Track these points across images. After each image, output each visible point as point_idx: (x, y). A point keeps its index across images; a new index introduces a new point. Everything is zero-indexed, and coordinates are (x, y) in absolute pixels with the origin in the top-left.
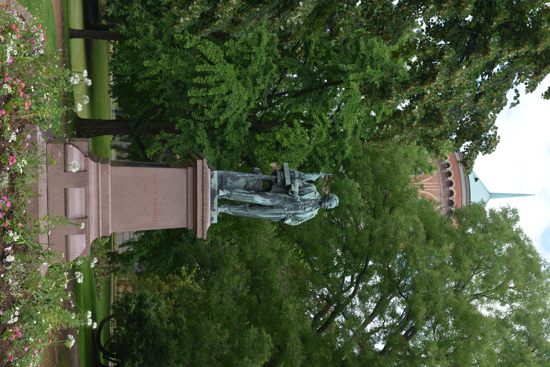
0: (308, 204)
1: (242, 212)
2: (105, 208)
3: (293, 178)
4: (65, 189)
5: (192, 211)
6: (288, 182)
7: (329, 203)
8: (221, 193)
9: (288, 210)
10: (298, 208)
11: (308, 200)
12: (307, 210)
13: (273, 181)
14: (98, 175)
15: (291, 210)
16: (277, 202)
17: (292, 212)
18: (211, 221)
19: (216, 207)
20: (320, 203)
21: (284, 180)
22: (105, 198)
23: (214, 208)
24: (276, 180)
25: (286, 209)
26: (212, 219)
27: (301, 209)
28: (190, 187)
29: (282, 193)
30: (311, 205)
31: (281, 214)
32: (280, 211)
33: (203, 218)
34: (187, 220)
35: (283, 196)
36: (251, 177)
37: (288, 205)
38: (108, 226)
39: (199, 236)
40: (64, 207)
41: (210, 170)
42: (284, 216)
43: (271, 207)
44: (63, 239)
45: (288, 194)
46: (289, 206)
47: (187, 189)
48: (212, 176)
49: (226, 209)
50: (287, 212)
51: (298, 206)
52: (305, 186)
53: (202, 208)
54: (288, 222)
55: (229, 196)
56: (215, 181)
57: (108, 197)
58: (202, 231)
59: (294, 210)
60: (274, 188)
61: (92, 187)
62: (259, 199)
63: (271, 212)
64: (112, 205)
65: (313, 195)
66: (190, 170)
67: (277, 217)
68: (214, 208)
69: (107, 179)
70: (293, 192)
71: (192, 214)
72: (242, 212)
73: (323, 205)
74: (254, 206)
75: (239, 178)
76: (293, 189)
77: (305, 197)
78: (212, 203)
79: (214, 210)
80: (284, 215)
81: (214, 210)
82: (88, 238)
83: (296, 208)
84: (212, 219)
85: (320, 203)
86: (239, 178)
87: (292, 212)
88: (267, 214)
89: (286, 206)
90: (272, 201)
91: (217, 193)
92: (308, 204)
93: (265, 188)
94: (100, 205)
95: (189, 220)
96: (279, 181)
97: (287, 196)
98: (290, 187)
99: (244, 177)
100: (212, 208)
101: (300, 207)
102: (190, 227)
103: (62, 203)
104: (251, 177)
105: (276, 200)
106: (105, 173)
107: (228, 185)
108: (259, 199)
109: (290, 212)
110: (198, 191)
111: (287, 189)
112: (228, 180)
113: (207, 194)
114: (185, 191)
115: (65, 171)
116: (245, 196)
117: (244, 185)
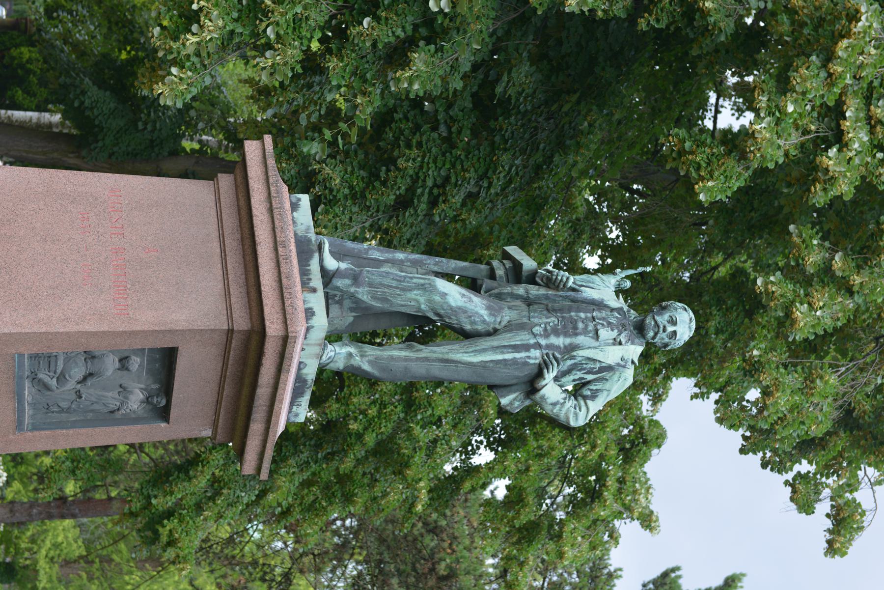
0: (604, 319)
1: (403, 353)
5: (242, 280)
7: (666, 316)
9: (546, 335)
10: (575, 328)
15: (556, 332)
17: (560, 341)
18: (308, 319)
23: (312, 284)
25: (537, 330)
27: (585, 332)
28: (230, 221)
30: (613, 321)
31: (527, 348)
33: (280, 281)
37: (541, 321)
41: (285, 188)
46: (545, 320)
47: (223, 251)
48: (295, 206)
50: (543, 342)
51: (574, 323)
53: (272, 256)
58: (280, 316)
59: (566, 335)
63: (495, 343)
66: (225, 181)
67: (514, 361)
68: (312, 284)
71: (243, 290)
78: (305, 273)
79: (314, 290)
80: (536, 353)
81: (314, 290)
87: (560, 341)
88: (484, 350)
89: (536, 320)
91: (315, 248)
92: (604, 319)
95: (235, 307)
101: (581, 325)
102: (242, 322)
105: (501, 309)
110: (255, 212)
116: (405, 277)
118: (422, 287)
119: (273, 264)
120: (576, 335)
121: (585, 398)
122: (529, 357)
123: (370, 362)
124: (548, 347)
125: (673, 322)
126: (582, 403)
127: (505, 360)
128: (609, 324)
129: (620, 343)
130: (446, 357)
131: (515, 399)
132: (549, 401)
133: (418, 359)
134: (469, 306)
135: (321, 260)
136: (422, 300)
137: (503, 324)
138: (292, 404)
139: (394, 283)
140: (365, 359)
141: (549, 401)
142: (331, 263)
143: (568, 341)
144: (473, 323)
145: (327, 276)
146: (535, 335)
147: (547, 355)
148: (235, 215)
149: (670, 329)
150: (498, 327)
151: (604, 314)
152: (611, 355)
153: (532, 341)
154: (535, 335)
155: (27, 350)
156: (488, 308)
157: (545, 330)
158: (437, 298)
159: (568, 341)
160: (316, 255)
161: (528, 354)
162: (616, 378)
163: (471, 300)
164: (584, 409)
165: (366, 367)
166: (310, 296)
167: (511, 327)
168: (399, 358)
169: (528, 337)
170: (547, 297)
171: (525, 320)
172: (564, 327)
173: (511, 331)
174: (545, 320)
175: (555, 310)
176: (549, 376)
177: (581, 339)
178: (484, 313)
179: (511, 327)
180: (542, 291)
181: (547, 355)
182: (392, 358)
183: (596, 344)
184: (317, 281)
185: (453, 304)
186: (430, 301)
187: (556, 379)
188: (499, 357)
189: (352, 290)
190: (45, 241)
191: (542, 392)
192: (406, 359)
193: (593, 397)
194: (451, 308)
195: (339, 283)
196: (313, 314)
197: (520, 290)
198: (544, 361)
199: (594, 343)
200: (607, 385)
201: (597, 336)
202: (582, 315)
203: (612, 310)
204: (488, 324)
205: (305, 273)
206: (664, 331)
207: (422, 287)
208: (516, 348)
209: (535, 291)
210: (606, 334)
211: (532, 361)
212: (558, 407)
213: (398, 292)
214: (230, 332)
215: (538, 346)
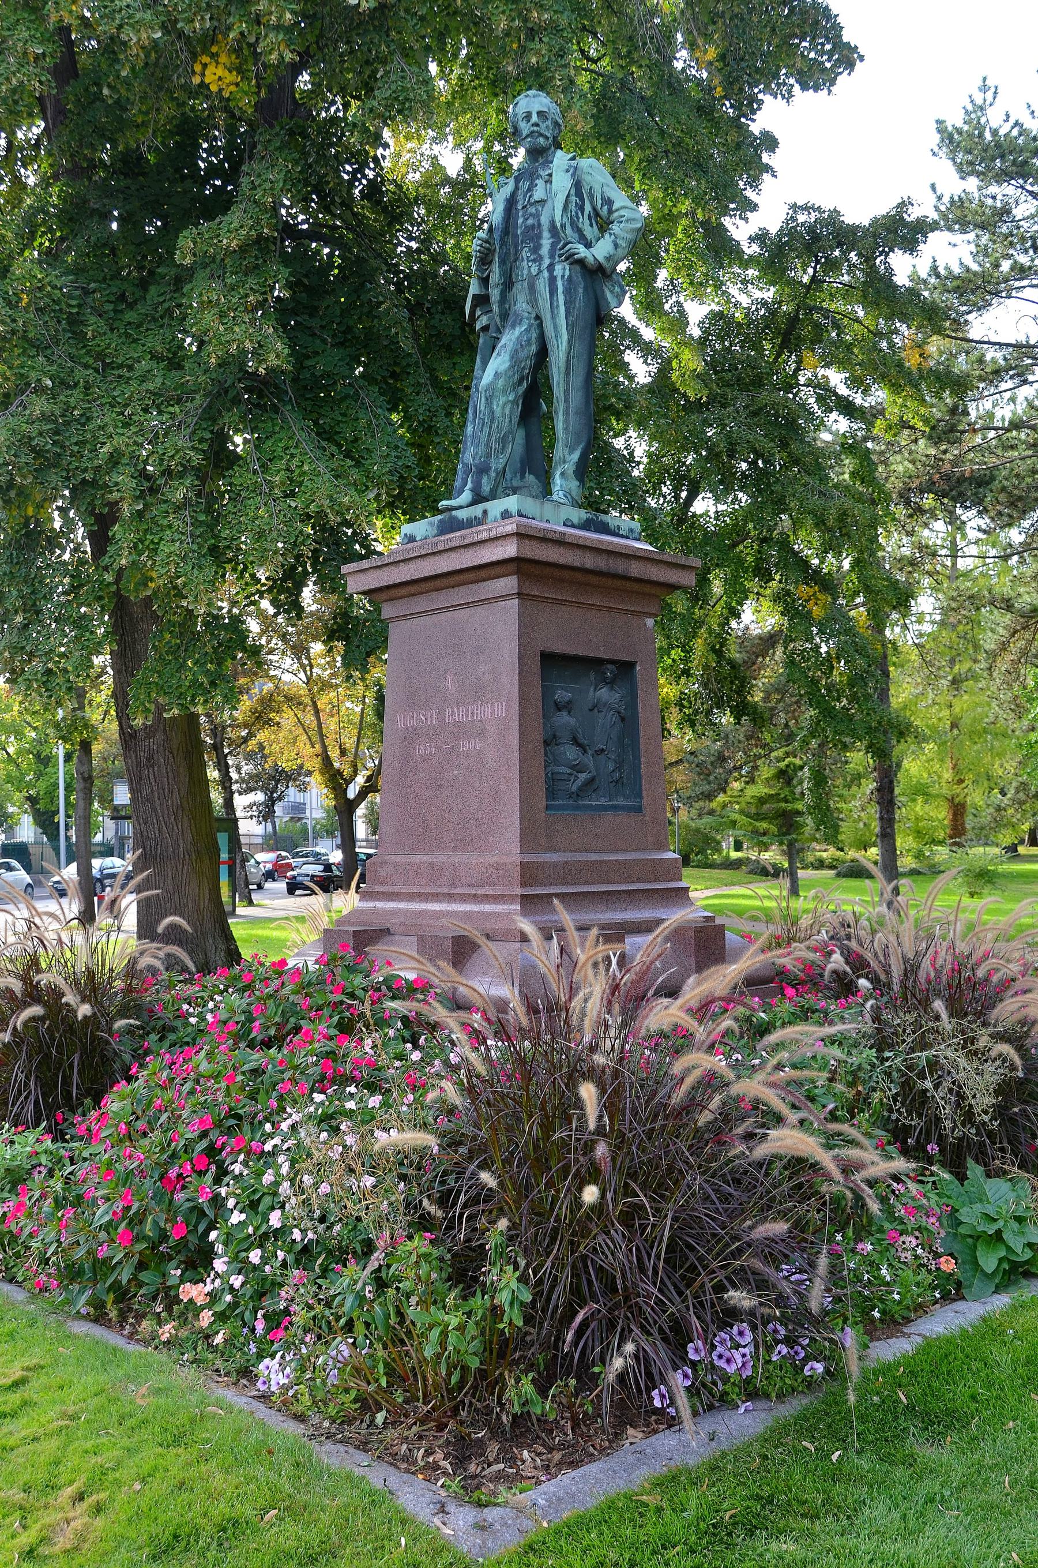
9: (539, 259)
17: (546, 243)
22: (434, 872)
27: (537, 216)
31: (552, 280)
32: (542, 286)
37: (526, 268)
50: (547, 262)
57: (432, 866)
59: (539, 237)
63: (549, 316)
67: (567, 292)
72: (561, 417)
78: (469, 524)
79: (485, 512)
81: (485, 512)
87: (546, 243)
89: (525, 272)
94: (445, 890)
101: (530, 222)
102: (508, 584)
109: (545, 250)
118: (489, 400)
119: (453, 555)
120: (539, 225)
121: (610, 212)
122: (563, 277)
123: (571, 452)
124: (552, 256)
125: (528, 116)
126: (616, 215)
127: (565, 303)
128: (530, 190)
129: (550, 175)
130: (563, 370)
131: (612, 292)
132: (612, 251)
133: (566, 401)
134: (510, 347)
135: (461, 507)
136: (503, 400)
137: (530, 309)
138: (618, 535)
139: (486, 430)
140: (568, 458)
141: (612, 251)
142: (466, 496)
143: (546, 234)
144: (529, 341)
146: (540, 271)
147: (560, 256)
148: (416, 599)
149: (534, 118)
150: (533, 315)
151: (520, 198)
152: (562, 184)
153: (546, 274)
154: (540, 271)
155: (541, 800)
156: (513, 327)
157: (534, 261)
158: (501, 382)
159: (546, 234)
160: (454, 513)
161: (559, 279)
162: (588, 178)
163: (504, 346)
164: (622, 212)
165: (576, 456)
166: (491, 515)
167: (533, 301)
168: (566, 422)
169: (541, 280)
170: (503, 262)
171: (525, 285)
172: (531, 240)
173: (536, 301)
174: (525, 262)
175: (516, 251)
176: (582, 251)
177: (545, 220)
178: (517, 331)
179: (533, 301)
180: (496, 268)
181: (560, 256)
182: (566, 429)
183: (550, 201)
184: (477, 510)
185: (507, 365)
186: (504, 391)
187: (588, 245)
188: (562, 309)
189: (493, 474)
190: (440, 786)
191: (601, 259)
192: (567, 413)
193: (609, 202)
194: (512, 367)
195: (486, 489)
196: (506, 511)
197: (495, 294)
198: (567, 259)
199: (548, 205)
200: (597, 188)
201: (542, 202)
202: (520, 221)
203: (517, 188)
204: (530, 326)
205: (469, 524)
206: (537, 125)
207: (489, 400)
208: (553, 291)
209: (495, 277)
210: (539, 194)
211: (567, 273)
212: (619, 241)
213: (494, 426)
214: (520, 595)
215: (551, 268)
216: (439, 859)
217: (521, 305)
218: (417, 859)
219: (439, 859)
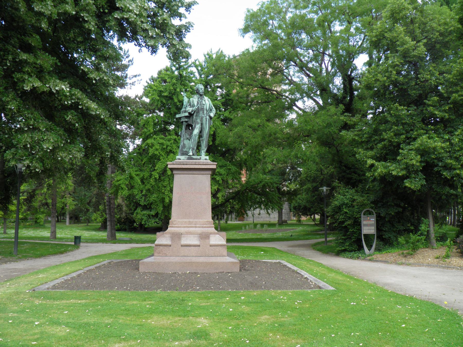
2: (190, 223)
3: (185, 112)
4: (182, 246)
6: (187, 114)
8: (191, 154)
9: (204, 114)
11: (198, 102)
12: (204, 103)
13: (186, 124)
14: (176, 227)
15: (203, 112)
16: (199, 121)
17: (205, 112)
19: (199, 157)
20: (201, 95)
21: (186, 117)
24: (186, 122)
25: (203, 116)
26: (206, 159)
27: (203, 106)
29: (193, 117)
31: (206, 118)
32: (204, 119)
34: (205, 174)
35: (194, 117)
36: (183, 136)
38: (207, 222)
39: (214, 167)
40: (192, 247)
42: (208, 117)
43: (202, 124)
44: (211, 247)
45: (193, 114)
48: (180, 159)
49: (203, 152)
52: (190, 105)
54: (212, 115)
55: (193, 149)
56: (183, 158)
57: (190, 221)
60: (190, 123)
61: (182, 230)
62: (196, 131)
64: (194, 219)
65: (195, 99)
69: (179, 221)
70: (192, 111)
73: (201, 93)
74: (200, 135)
75: (184, 144)
76: (190, 111)
77: (196, 104)
78: (196, 159)
79: (200, 158)
81: (200, 158)
82: (214, 233)
83: (203, 109)
84: (206, 159)
85: (201, 95)
86: (184, 144)
87: (205, 112)
90: (198, 124)
93: (190, 127)
96: (186, 120)
97: (195, 115)
98: (189, 113)
99: (183, 141)
100: (199, 159)
102: (210, 172)
103: (190, 248)
104: (183, 136)
106: (175, 223)
107: (188, 150)
108: (196, 131)
109: (205, 113)
111: (191, 115)
112: (185, 150)
113: (189, 162)
114: (188, 175)
115: (170, 246)
117: (188, 141)
145: (193, 155)
166: (202, 159)
177: (205, 107)
205: (196, 159)
208: (206, 120)
216: (191, 220)
217: (199, 121)
218: (185, 220)
219: (191, 220)
